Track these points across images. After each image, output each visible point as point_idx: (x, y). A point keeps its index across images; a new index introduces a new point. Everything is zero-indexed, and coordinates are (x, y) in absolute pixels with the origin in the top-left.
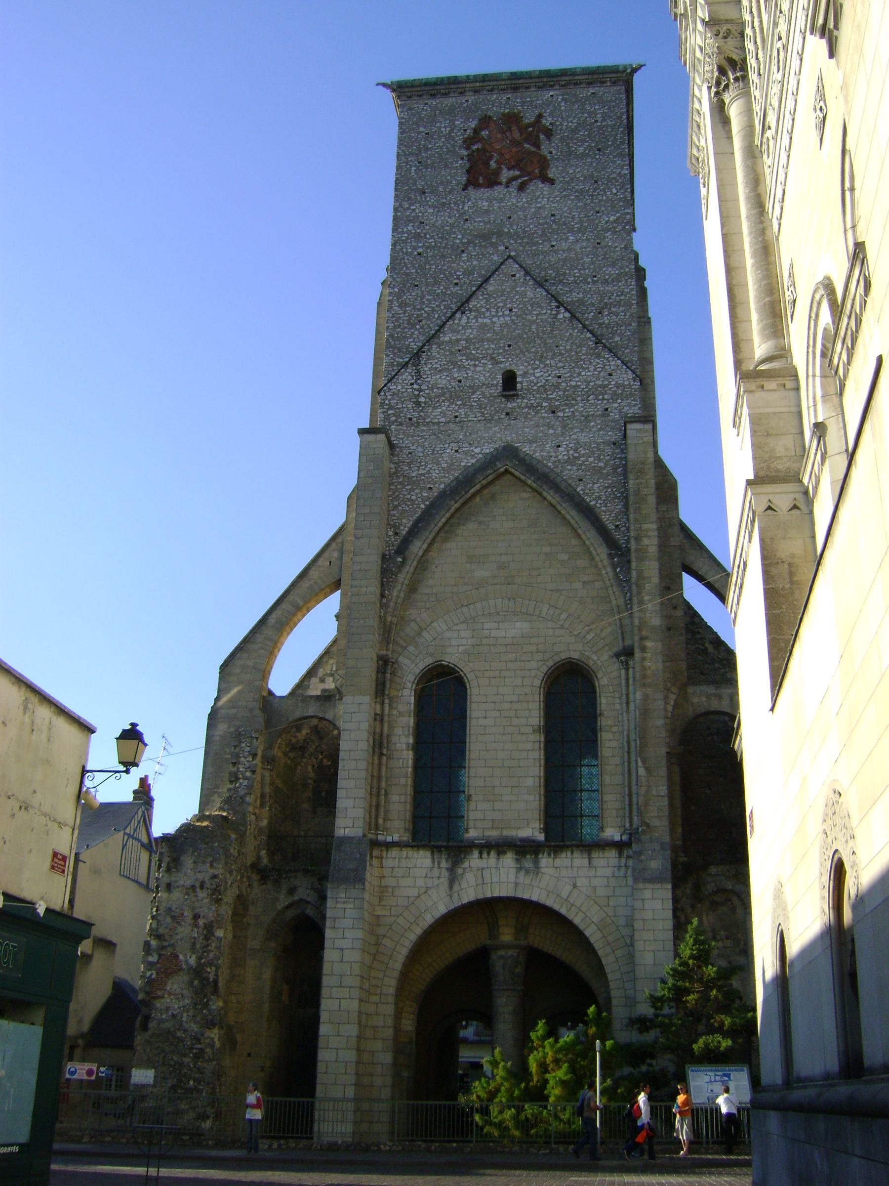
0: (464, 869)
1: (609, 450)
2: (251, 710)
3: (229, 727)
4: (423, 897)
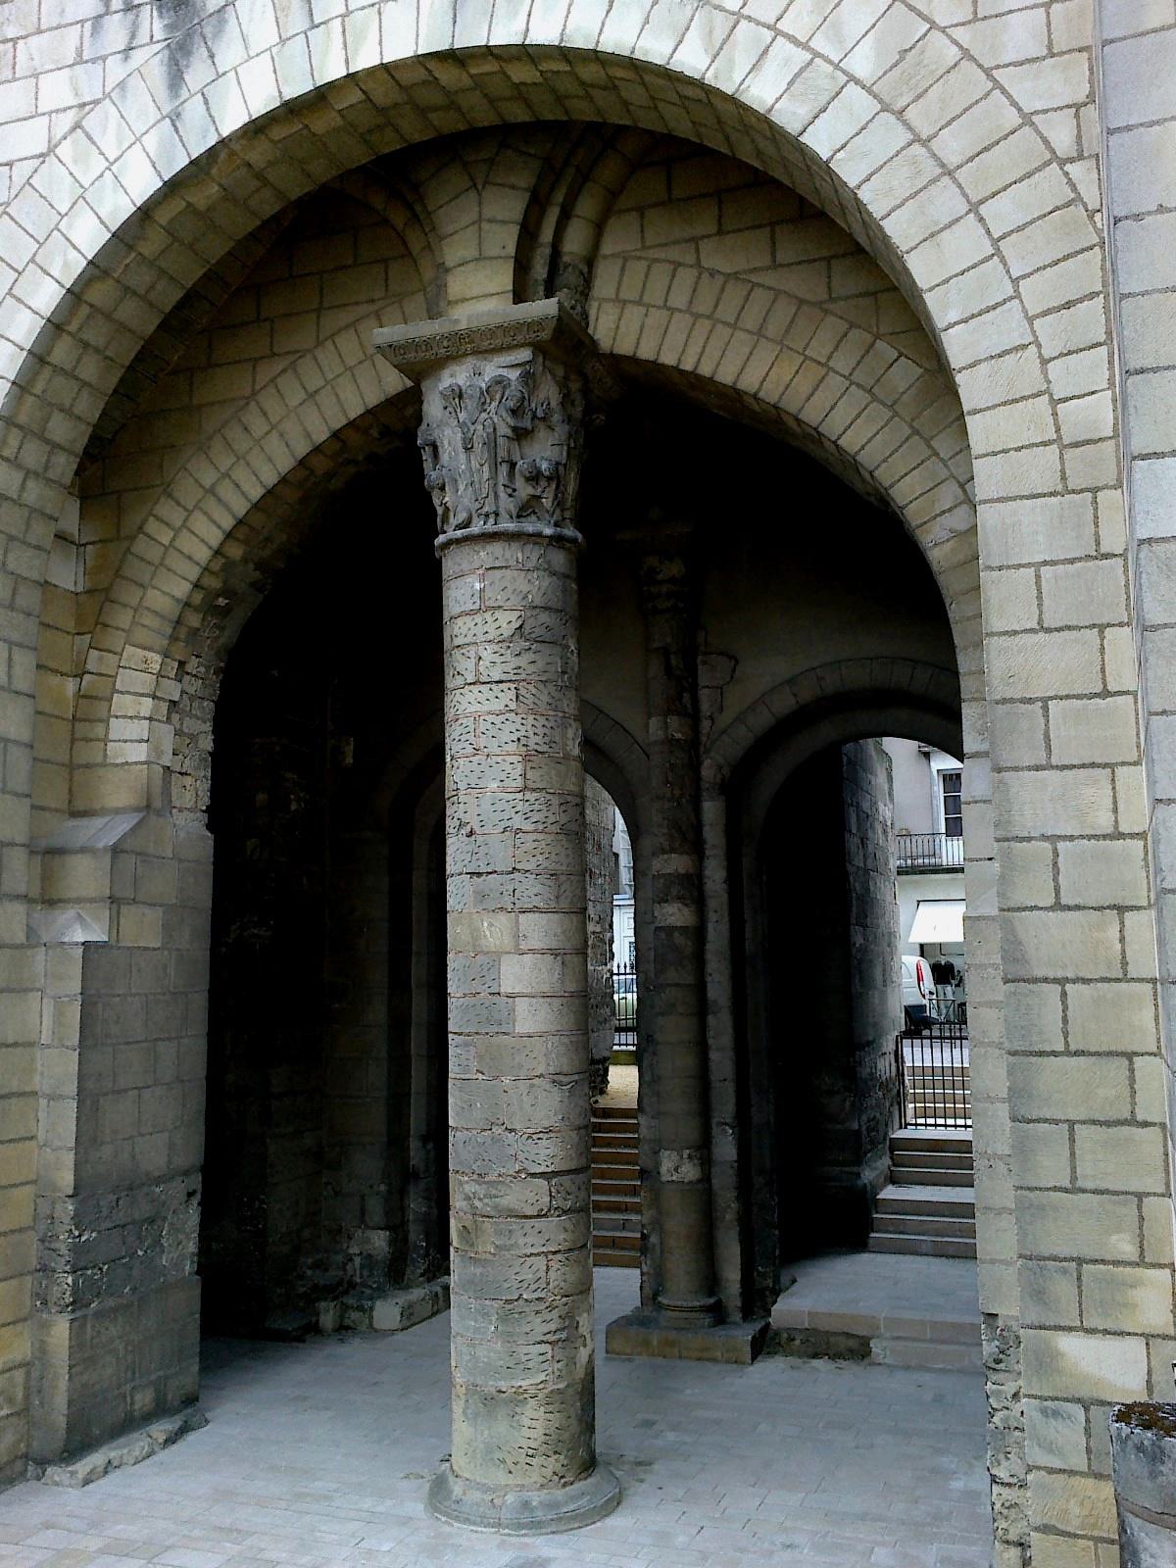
4: (65, 150)
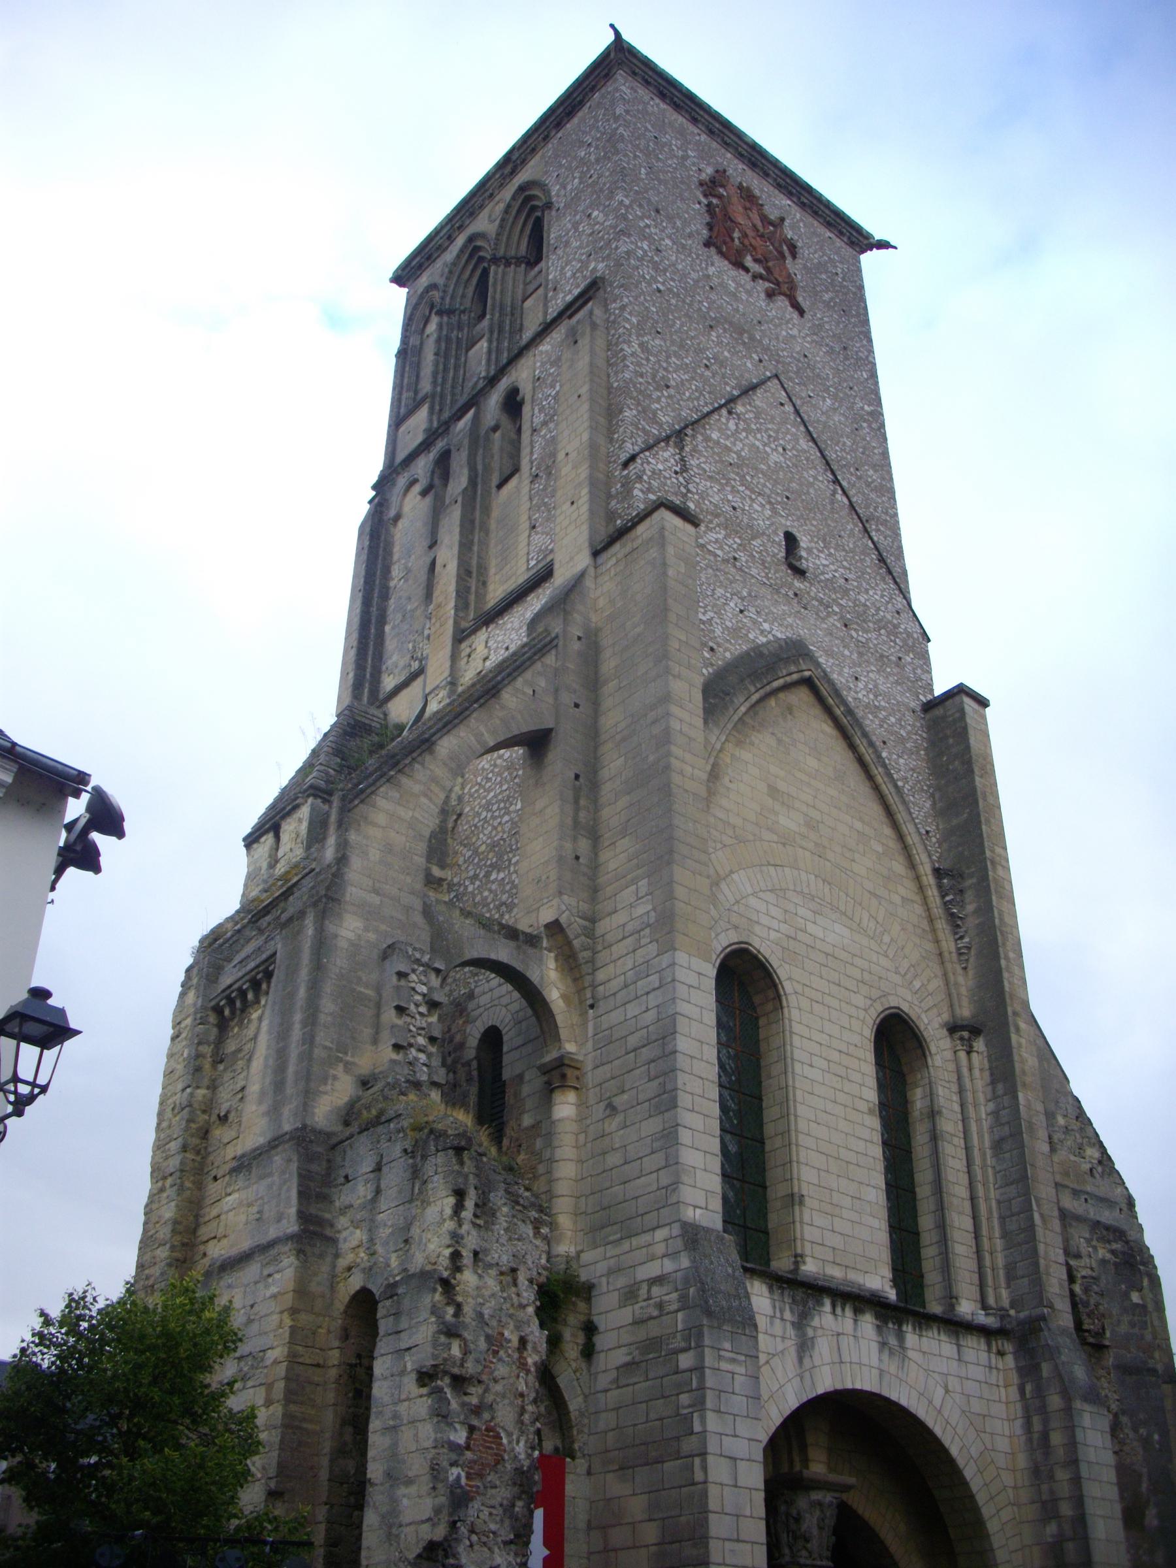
0: (815, 1329)
1: (909, 717)
2: (408, 909)
3: (366, 929)
